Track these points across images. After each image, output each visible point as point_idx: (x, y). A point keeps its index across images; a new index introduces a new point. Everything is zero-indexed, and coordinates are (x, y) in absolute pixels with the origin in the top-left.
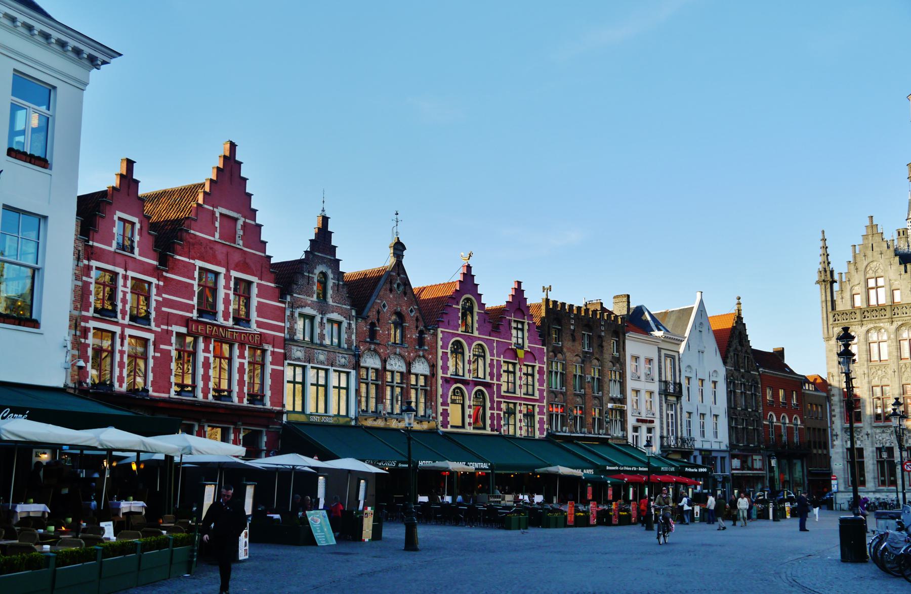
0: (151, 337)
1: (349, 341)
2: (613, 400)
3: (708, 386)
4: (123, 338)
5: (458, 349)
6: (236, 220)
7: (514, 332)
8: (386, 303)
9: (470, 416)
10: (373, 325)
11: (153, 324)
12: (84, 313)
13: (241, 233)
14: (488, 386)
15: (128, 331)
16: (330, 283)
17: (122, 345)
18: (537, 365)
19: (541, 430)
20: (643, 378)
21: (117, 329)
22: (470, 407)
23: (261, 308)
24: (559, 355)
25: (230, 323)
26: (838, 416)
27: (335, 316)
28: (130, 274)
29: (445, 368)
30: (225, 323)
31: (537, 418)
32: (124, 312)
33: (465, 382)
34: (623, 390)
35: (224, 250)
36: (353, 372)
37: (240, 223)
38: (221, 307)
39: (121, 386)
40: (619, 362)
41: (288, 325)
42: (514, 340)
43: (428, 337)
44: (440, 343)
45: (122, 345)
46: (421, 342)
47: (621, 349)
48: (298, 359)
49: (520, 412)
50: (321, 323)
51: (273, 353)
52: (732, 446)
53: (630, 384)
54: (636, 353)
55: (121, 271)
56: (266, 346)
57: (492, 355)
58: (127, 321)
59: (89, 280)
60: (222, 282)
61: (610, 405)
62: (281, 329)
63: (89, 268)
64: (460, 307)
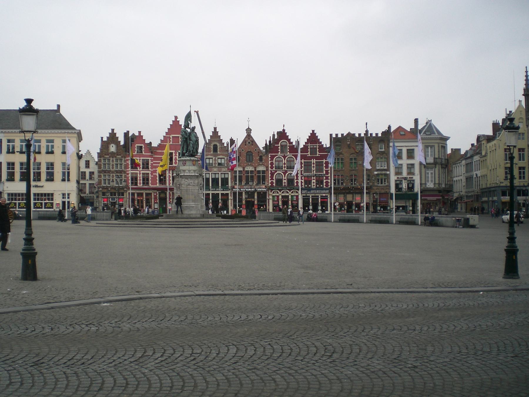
4: (140, 174)
9: (285, 183)
11: (150, 169)
15: (141, 172)
19: (327, 185)
21: (138, 172)
22: (285, 179)
24: (341, 155)
31: (325, 181)
36: (229, 173)
38: (174, 161)
46: (261, 159)
47: (386, 148)
49: (314, 179)
50: (215, 160)
58: (141, 169)
60: (174, 154)
61: (376, 173)
64: (279, 145)
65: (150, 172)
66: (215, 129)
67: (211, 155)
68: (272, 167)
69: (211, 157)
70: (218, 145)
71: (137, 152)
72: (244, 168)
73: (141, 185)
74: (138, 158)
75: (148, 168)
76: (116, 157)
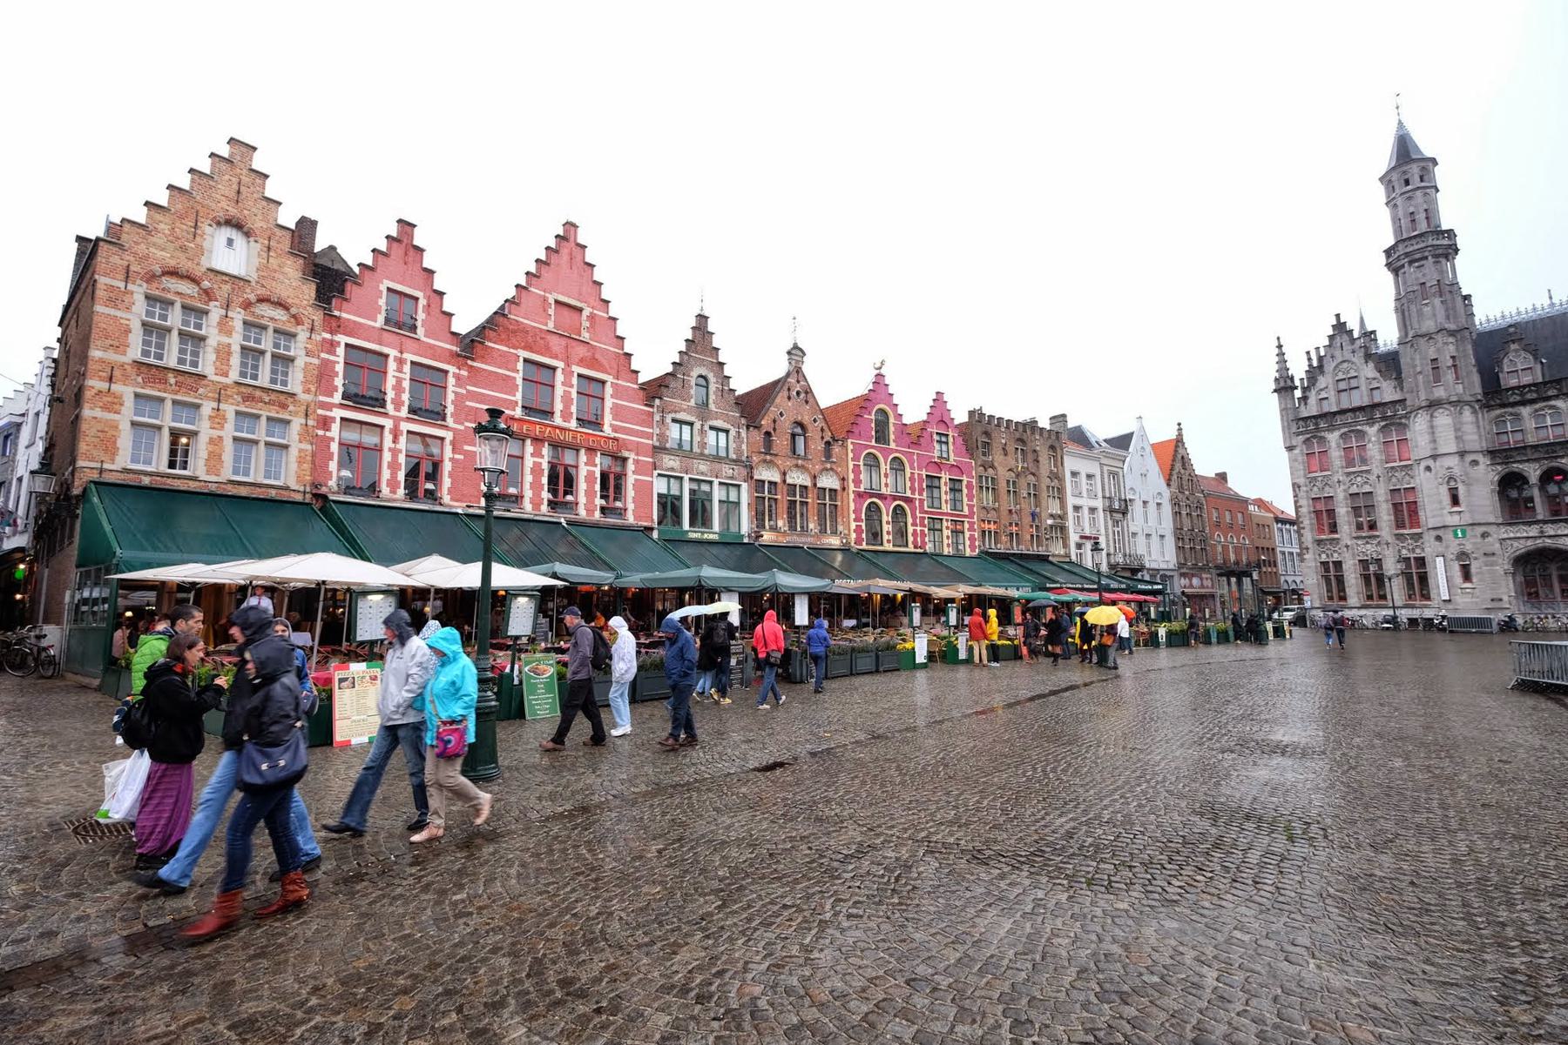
0: (449, 436)
1: (738, 451)
2: (1052, 516)
3: (1152, 507)
5: (872, 463)
6: (580, 310)
7: (937, 446)
8: (783, 410)
10: (768, 434)
11: (450, 421)
12: (321, 398)
13: (586, 324)
14: (909, 500)
15: (405, 427)
16: (712, 387)
17: (395, 440)
18: (965, 478)
19: (972, 547)
20: (1085, 494)
23: (617, 412)
25: (573, 424)
26: (1308, 528)
27: (719, 423)
28: (409, 357)
29: (857, 482)
30: (565, 425)
31: (967, 534)
32: (398, 404)
33: (882, 497)
34: (1063, 506)
35: (563, 342)
36: (744, 486)
37: (586, 312)
39: (393, 491)
40: (1057, 476)
41: (657, 431)
42: (937, 454)
43: (836, 449)
44: (851, 455)
45: (395, 440)
48: (672, 469)
50: (702, 431)
51: (636, 462)
52: (1181, 565)
53: (1071, 501)
54: (1075, 469)
55: (393, 353)
56: (626, 454)
57: (912, 468)
58: (404, 412)
59: (332, 358)
61: (1050, 522)
62: (650, 436)
63: (331, 346)
65: (449, 436)
66: (702, 319)
67: (688, 410)
68: (857, 482)
69: (691, 419)
70: (711, 376)
71: (387, 321)
72: (784, 474)
73: (401, 492)
74: (393, 353)
75: (438, 415)
76: (247, 305)
